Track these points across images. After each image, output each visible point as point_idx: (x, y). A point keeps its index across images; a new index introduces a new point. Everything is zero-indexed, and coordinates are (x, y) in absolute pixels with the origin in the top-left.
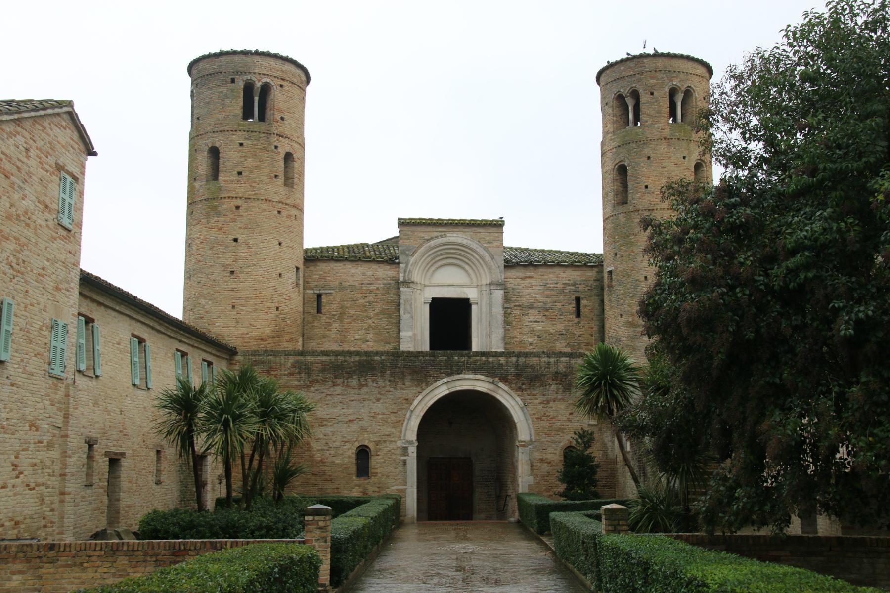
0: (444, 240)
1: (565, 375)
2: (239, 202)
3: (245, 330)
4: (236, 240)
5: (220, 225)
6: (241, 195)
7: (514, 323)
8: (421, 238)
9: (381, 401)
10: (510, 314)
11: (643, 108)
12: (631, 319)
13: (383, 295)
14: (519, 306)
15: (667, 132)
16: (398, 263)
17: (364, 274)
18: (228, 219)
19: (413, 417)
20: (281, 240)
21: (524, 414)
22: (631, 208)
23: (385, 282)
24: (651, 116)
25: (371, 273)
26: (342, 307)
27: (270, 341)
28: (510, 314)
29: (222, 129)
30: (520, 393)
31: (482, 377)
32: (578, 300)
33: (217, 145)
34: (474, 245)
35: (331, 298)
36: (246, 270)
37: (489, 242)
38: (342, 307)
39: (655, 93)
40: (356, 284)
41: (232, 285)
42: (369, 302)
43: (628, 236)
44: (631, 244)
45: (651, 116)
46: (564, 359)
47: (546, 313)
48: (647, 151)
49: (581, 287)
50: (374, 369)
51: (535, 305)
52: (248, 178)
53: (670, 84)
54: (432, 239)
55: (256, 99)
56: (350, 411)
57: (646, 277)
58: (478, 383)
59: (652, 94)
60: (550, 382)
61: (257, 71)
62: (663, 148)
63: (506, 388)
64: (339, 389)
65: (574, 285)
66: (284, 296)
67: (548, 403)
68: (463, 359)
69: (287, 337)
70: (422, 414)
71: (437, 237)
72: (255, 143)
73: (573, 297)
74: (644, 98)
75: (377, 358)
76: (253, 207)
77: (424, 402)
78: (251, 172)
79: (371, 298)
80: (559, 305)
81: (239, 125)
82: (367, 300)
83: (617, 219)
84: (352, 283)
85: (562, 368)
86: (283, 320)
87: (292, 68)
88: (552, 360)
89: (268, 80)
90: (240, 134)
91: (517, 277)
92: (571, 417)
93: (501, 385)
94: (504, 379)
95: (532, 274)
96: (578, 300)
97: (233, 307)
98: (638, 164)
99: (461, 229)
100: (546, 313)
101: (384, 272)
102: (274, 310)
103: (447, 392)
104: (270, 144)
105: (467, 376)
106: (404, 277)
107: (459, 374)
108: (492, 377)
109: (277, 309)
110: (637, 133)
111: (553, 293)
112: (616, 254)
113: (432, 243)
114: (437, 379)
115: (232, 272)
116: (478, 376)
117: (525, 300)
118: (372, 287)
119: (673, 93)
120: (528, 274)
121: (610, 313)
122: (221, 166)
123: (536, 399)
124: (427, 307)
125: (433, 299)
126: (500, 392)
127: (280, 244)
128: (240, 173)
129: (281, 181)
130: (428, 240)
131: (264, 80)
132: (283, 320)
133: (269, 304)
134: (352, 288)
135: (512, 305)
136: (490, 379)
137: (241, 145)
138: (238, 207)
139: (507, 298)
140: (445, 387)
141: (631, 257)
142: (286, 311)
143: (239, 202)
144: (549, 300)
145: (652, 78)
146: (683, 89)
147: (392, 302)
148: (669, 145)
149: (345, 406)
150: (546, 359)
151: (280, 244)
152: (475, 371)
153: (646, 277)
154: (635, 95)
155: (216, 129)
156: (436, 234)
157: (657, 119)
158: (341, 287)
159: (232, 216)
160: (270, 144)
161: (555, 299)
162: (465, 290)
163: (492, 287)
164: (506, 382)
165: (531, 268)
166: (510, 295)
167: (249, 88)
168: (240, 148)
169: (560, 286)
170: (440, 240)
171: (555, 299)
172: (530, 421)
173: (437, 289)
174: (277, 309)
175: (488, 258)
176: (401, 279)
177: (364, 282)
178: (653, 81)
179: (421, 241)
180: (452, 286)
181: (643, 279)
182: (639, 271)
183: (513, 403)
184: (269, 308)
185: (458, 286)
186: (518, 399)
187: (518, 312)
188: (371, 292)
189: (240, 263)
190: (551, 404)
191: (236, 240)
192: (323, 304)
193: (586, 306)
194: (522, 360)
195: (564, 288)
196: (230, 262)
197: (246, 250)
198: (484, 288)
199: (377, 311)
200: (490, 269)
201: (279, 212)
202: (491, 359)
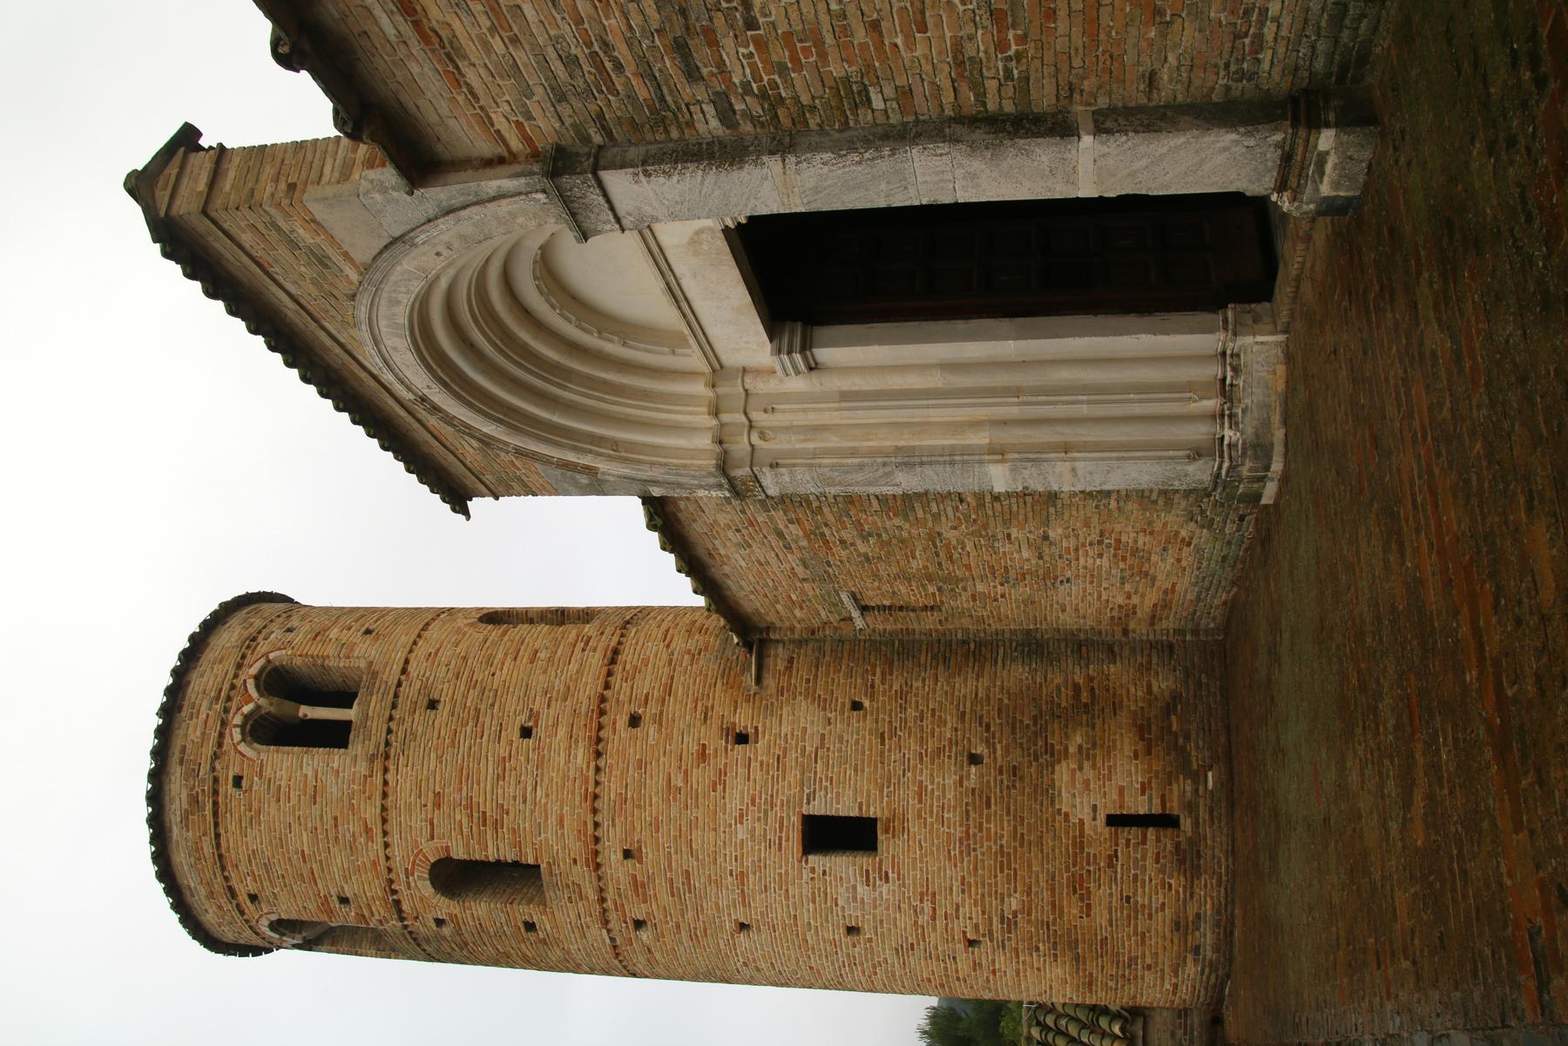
0: (439, 396)
7: (836, 69)
14: (681, 49)
20: (729, 926)
27: (1092, 967)
66: (924, 919)
69: (1072, 909)
86: (1009, 924)
87: (181, 859)
109: (972, 943)
113: (489, 429)
132: (1009, 924)
133: (963, 966)
142: (978, 917)
151: (743, 927)
184: (976, 966)
201: (639, 924)
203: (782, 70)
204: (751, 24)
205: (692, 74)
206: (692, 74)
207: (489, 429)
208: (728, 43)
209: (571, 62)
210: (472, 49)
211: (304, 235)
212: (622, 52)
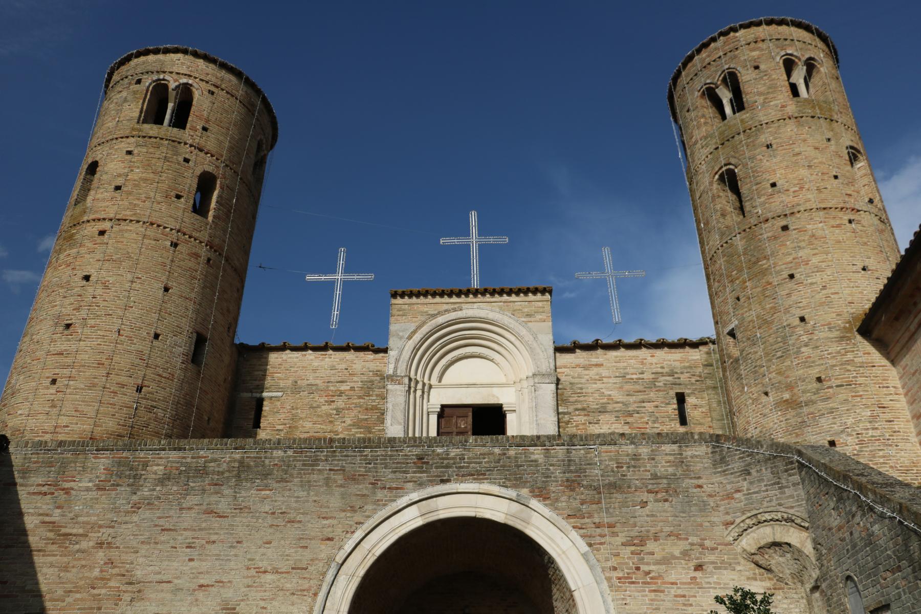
0: (460, 314)
1: (673, 479)
2: (106, 225)
3: (63, 421)
4: (87, 278)
5: (70, 259)
6: (112, 216)
8: (422, 313)
9: (274, 544)
10: (568, 422)
11: (745, 88)
12: (787, 396)
13: (360, 397)
14: (584, 409)
15: (792, 107)
16: (385, 351)
17: (333, 368)
18: (83, 250)
19: (342, 579)
21: (592, 568)
22: (753, 221)
23: (365, 378)
24: (760, 94)
25: (344, 366)
26: (294, 418)
28: (568, 422)
29: (111, 137)
30: (579, 522)
31: (495, 489)
32: (681, 399)
33: (97, 159)
34: (505, 319)
35: (278, 404)
36: (92, 322)
37: (528, 315)
38: (294, 418)
39: (762, 67)
40: (318, 382)
41: (61, 346)
42: (337, 409)
43: (758, 260)
44: (764, 272)
45: (760, 94)
46: (668, 448)
47: (629, 420)
48: (764, 138)
49: (684, 378)
50: (266, 475)
51: (610, 407)
52: (130, 193)
53: (783, 53)
54: (440, 313)
55: (170, 106)
56: (205, 566)
57: (802, 319)
58: (489, 503)
59: (757, 68)
60: (645, 496)
61: (175, 69)
62: (790, 129)
63: (546, 511)
64: (188, 519)
65: (672, 374)
67: (642, 543)
68: (454, 452)
70: (362, 572)
71: (447, 311)
72: (151, 150)
73: (672, 393)
74: (746, 77)
75: (279, 453)
76: (127, 231)
77: (366, 545)
78: (135, 185)
79: (340, 403)
80: (649, 407)
81: (133, 129)
82: (334, 406)
83: (732, 245)
84: (313, 382)
85: (663, 467)
88: (644, 450)
89: (190, 82)
90: (131, 140)
91: (578, 366)
92: (698, 574)
93: (534, 503)
94: (542, 494)
95: (600, 360)
96: (681, 399)
97: (54, 382)
98: (752, 158)
99: (488, 297)
100: (629, 420)
101: (362, 362)
102: (132, 391)
103: (419, 522)
104: (177, 154)
105: (462, 487)
106: (396, 368)
107: (443, 481)
108: (515, 487)
110: (742, 121)
111: (638, 387)
112: (738, 299)
114: (397, 491)
115: (68, 326)
116: (486, 487)
117: (592, 401)
118: (344, 387)
119: (789, 65)
120: (594, 361)
121: (743, 398)
122: (95, 181)
123: (614, 534)
124: (434, 419)
125: (443, 407)
126: (536, 519)
127: (166, 289)
128: (118, 188)
129: (185, 204)
130: (434, 316)
131: (184, 80)
133: (123, 379)
134: (312, 389)
135: (571, 409)
136: (512, 493)
137: (129, 153)
138: (102, 233)
139: (560, 399)
140: (413, 511)
141: (768, 293)
143: (106, 225)
144: (632, 399)
145: (752, 50)
146: (804, 59)
147: (374, 408)
148: (800, 125)
149: (194, 553)
150: (630, 449)
152: (478, 475)
153: (802, 319)
154: (732, 81)
155: (103, 140)
156: (445, 307)
157: (772, 96)
158: (296, 388)
159: (90, 245)
160: (177, 154)
161: (641, 397)
162: (495, 391)
163: (536, 380)
164: (545, 499)
165: (600, 351)
166: (568, 393)
167: (160, 92)
168: (129, 157)
169: (648, 376)
170: (453, 316)
171: (641, 397)
172: (605, 585)
173: (450, 391)
174: (139, 389)
175: (529, 337)
176: (391, 372)
177: (332, 379)
178: (755, 54)
179: (423, 319)
180: (474, 385)
181: (797, 321)
182: (787, 311)
183: (565, 543)
184: (123, 386)
185: (482, 385)
186: (574, 534)
187: (582, 419)
188: (341, 394)
189: (84, 313)
190: (651, 546)
191: (87, 278)
192: (264, 413)
193: (696, 406)
194: (579, 452)
195: (655, 380)
196: (68, 310)
197: (99, 291)
198: (525, 384)
199: (349, 422)
200: (531, 351)
201: (175, 245)
202: (512, 452)
203: (577, 426)
204: (590, 423)
205: (577, 410)
206: (577, 410)
207: (441, 320)
208: (586, 418)
209: (581, 389)
210: (587, 372)
211: (539, 317)
212: (582, 399)
